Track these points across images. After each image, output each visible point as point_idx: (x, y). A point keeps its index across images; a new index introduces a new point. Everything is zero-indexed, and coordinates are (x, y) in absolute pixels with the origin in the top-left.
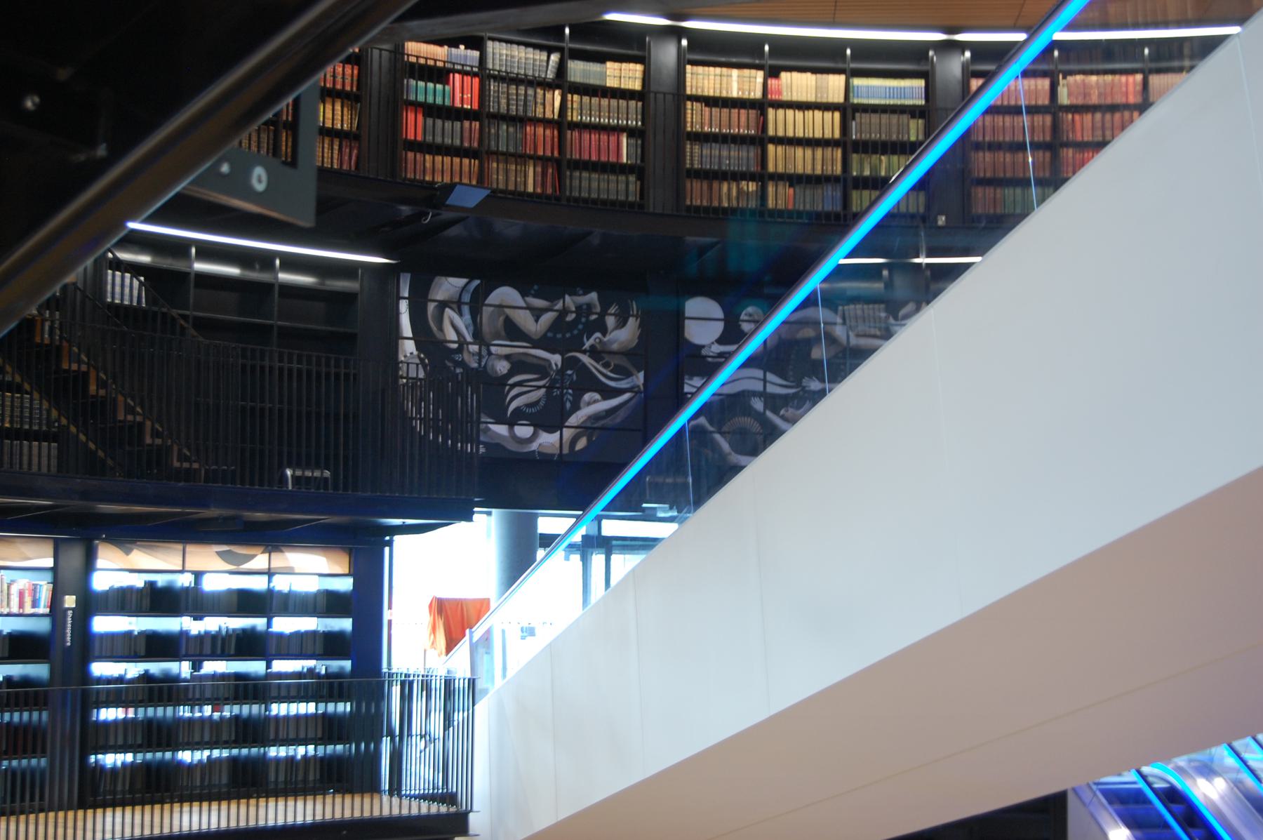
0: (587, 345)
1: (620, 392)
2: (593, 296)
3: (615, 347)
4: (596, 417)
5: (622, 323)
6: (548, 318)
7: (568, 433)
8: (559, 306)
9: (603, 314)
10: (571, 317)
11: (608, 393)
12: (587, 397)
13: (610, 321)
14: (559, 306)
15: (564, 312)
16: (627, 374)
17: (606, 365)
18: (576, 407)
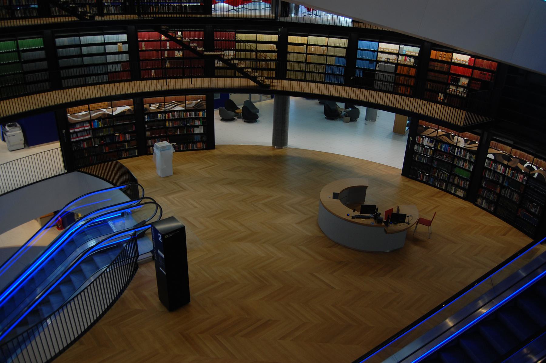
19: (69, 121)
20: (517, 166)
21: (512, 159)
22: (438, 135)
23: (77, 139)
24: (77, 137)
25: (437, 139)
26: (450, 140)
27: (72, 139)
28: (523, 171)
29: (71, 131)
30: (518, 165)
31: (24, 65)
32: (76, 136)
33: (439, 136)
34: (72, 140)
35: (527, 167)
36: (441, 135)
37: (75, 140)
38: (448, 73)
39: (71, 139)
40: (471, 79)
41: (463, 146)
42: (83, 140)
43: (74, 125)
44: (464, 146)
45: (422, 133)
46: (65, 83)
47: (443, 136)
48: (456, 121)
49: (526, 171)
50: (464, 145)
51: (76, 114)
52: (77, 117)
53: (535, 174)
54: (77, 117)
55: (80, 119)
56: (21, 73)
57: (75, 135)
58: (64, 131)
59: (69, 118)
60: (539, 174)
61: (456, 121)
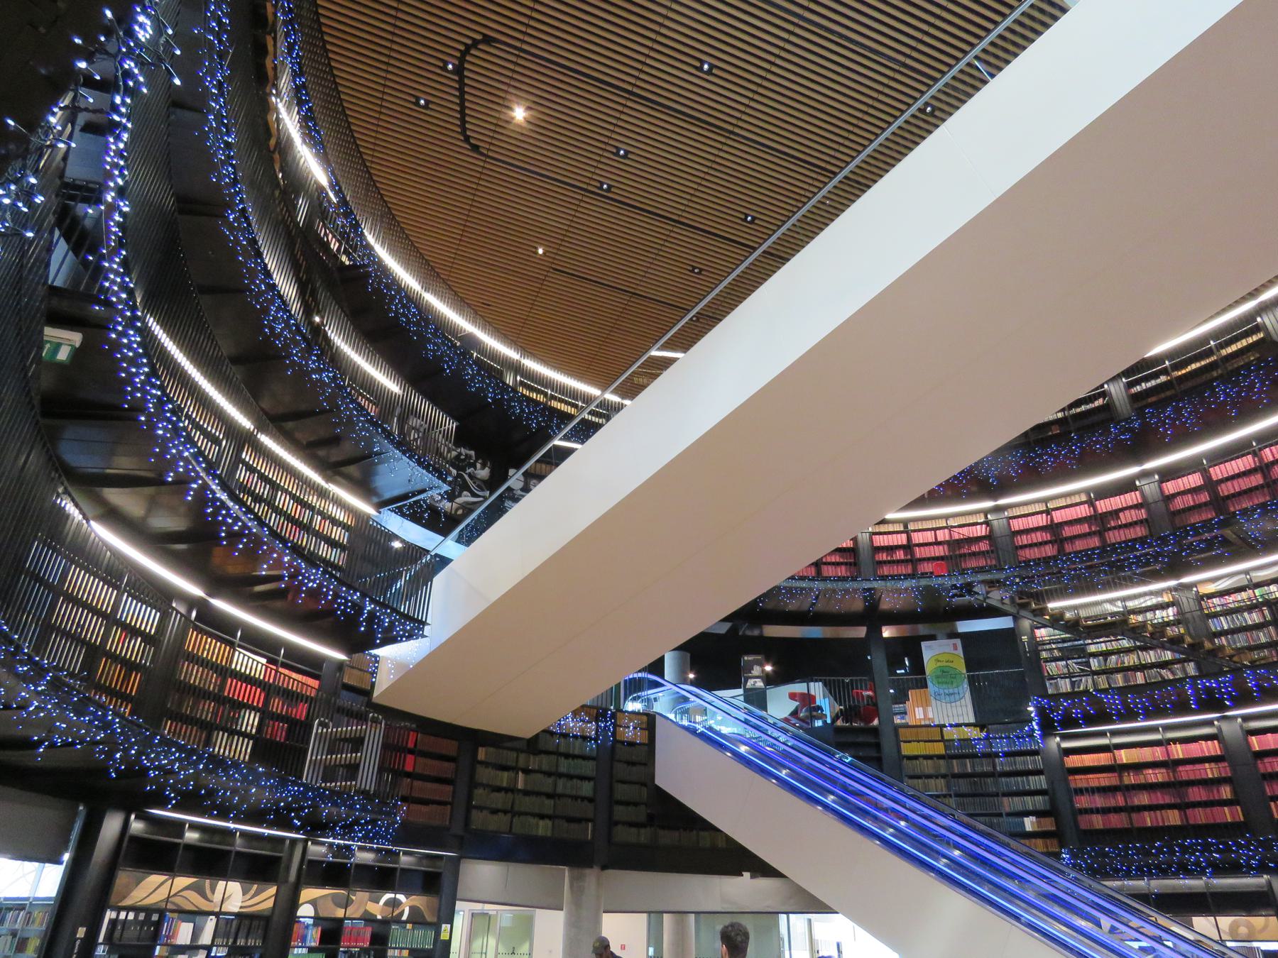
0: (468, 471)
1: (479, 496)
2: (472, 453)
3: (479, 477)
4: (468, 503)
5: (483, 466)
6: (454, 453)
7: (455, 505)
8: (459, 450)
9: (476, 461)
10: (463, 457)
11: (474, 495)
12: (465, 493)
13: (478, 466)
14: (459, 450)
15: (460, 454)
16: (483, 490)
17: (474, 483)
18: (460, 496)
20: (366, 910)
21: (354, 898)
22: (172, 894)
25: (170, 906)
26: (203, 900)
28: (379, 917)
30: (367, 908)
33: (175, 895)
35: (386, 904)
36: (180, 889)
38: (219, 699)
40: (265, 714)
41: (236, 906)
44: (241, 907)
45: (125, 897)
47: (184, 893)
49: (384, 915)
50: (240, 904)
53: (403, 912)
60: (412, 908)
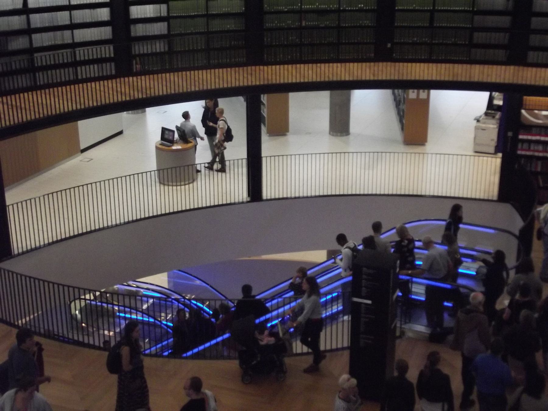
19: (522, 119)
23: (528, 153)
24: (529, 150)
27: (520, 150)
29: (521, 137)
31: (476, 18)
32: (528, 148)
34: (519, 152)
37: (523, 153)
39: (517, 149)
42: (539, 158)
43: (529, 128)
46: (532, 56)
48: (146, 82)
51: (536, 112)
52: (536, 117)
54: (536, 117)
55: (540, 122)
56: (469, 28)
57: (525, 146)
58: (510, 134)
59: (524, 116)
61: (146, 82)
